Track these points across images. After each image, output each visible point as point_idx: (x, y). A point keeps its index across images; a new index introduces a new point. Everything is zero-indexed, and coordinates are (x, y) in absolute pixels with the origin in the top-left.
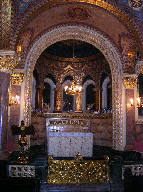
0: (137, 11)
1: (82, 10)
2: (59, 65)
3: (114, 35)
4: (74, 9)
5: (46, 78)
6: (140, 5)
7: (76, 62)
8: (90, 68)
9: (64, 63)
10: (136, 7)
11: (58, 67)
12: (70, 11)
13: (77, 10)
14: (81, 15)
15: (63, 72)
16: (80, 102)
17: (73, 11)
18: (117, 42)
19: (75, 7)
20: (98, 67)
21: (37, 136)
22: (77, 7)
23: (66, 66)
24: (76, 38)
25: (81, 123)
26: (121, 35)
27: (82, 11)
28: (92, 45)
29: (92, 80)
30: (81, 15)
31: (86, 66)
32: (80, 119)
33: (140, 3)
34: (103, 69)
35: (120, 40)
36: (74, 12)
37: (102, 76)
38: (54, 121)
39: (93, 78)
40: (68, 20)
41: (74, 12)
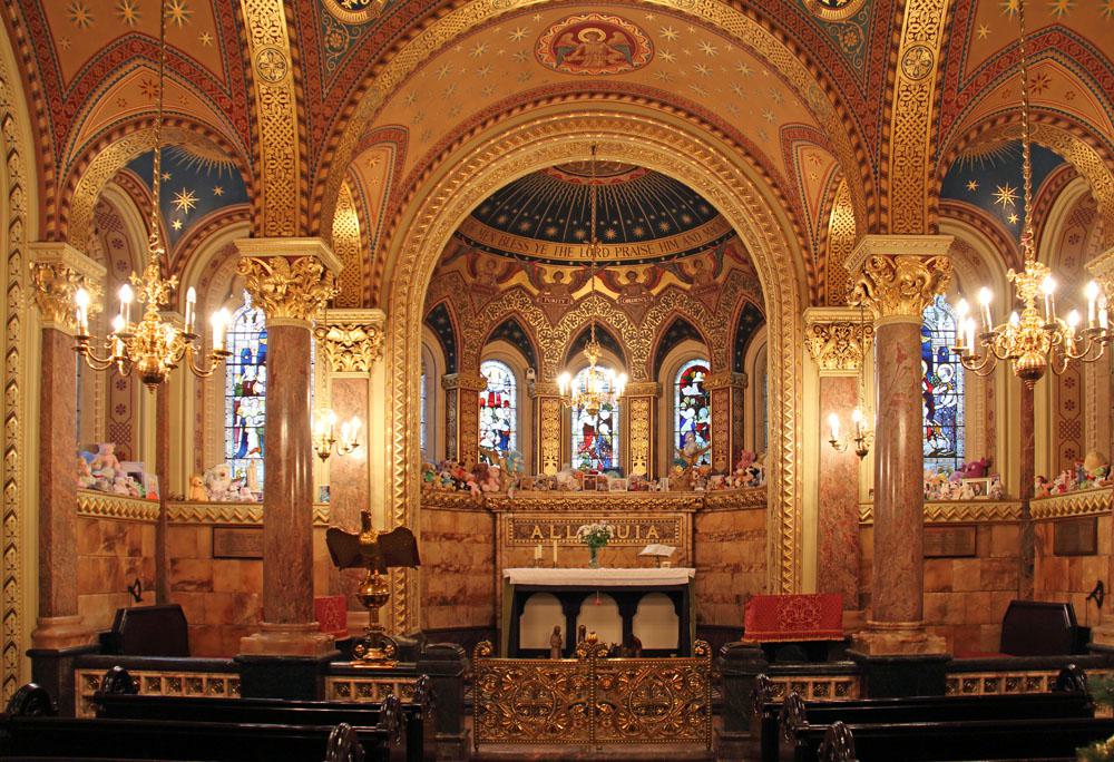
0: (837, 25)
1: (610, 30)
2: (548, 279)
4: (575, 30)
5: (493, 338)
7: (624, 263)
8: (688, 287)
9: (568, 271)
11: (541, 286)
12: (558, 38)
13: (591, 30)
14: (608, 53)
15: (569, 309)
16: (645, 444)
17: (571, 35)
18: (779, 165)
19: (574, 21)
20: (720, 279)
21: (460, 591)
22: (583, 18)
23: (579, 282)
24: (601, 157)
25: (650, 533)
26: (790, 135)
27: (609, 36)
30: (608, 53)
31: (669, 278)
32: (645, 516)
34: (741, 290)
35: (788, 158)
36: (576, 39)
38: (532, 528)
40: (555, 79)
41: (580, 42)
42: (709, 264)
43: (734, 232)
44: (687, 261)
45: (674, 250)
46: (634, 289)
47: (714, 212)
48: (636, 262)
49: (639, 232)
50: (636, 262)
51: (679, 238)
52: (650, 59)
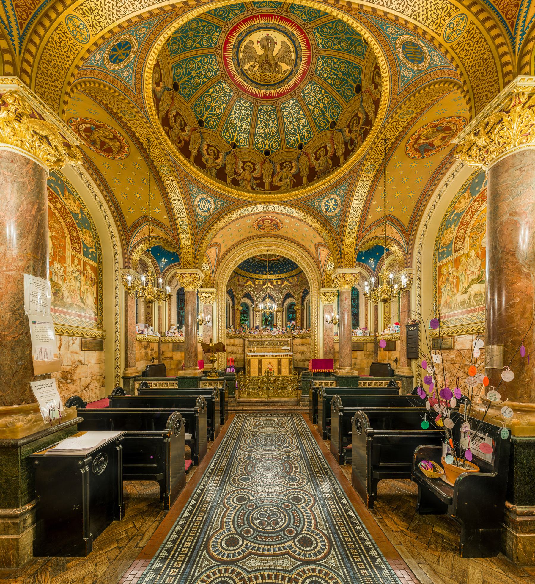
0: (332, 217)
1: (272, 220)
3: (311, 247)
6: (335, 209)
10: (331, 211)
18: (314, 254)
19: (263, 218)
20: (298, 283)
24: (269, 253)
26: (318, 246)
28: (289, 259)
29: (293, 297)
33: (335, 207)
35: (317, 252)
37: (304, 293)
39: (294, 295)
42: (296, 279)
43: (302, 271)
44: (290, 279)
45: (287, 276)
46: (277, 286)
47: (297, 266)
48: (278, 279)
49: (279, 272)
50: (278, 279)
51: (288, 273)
52: (282, 228)
